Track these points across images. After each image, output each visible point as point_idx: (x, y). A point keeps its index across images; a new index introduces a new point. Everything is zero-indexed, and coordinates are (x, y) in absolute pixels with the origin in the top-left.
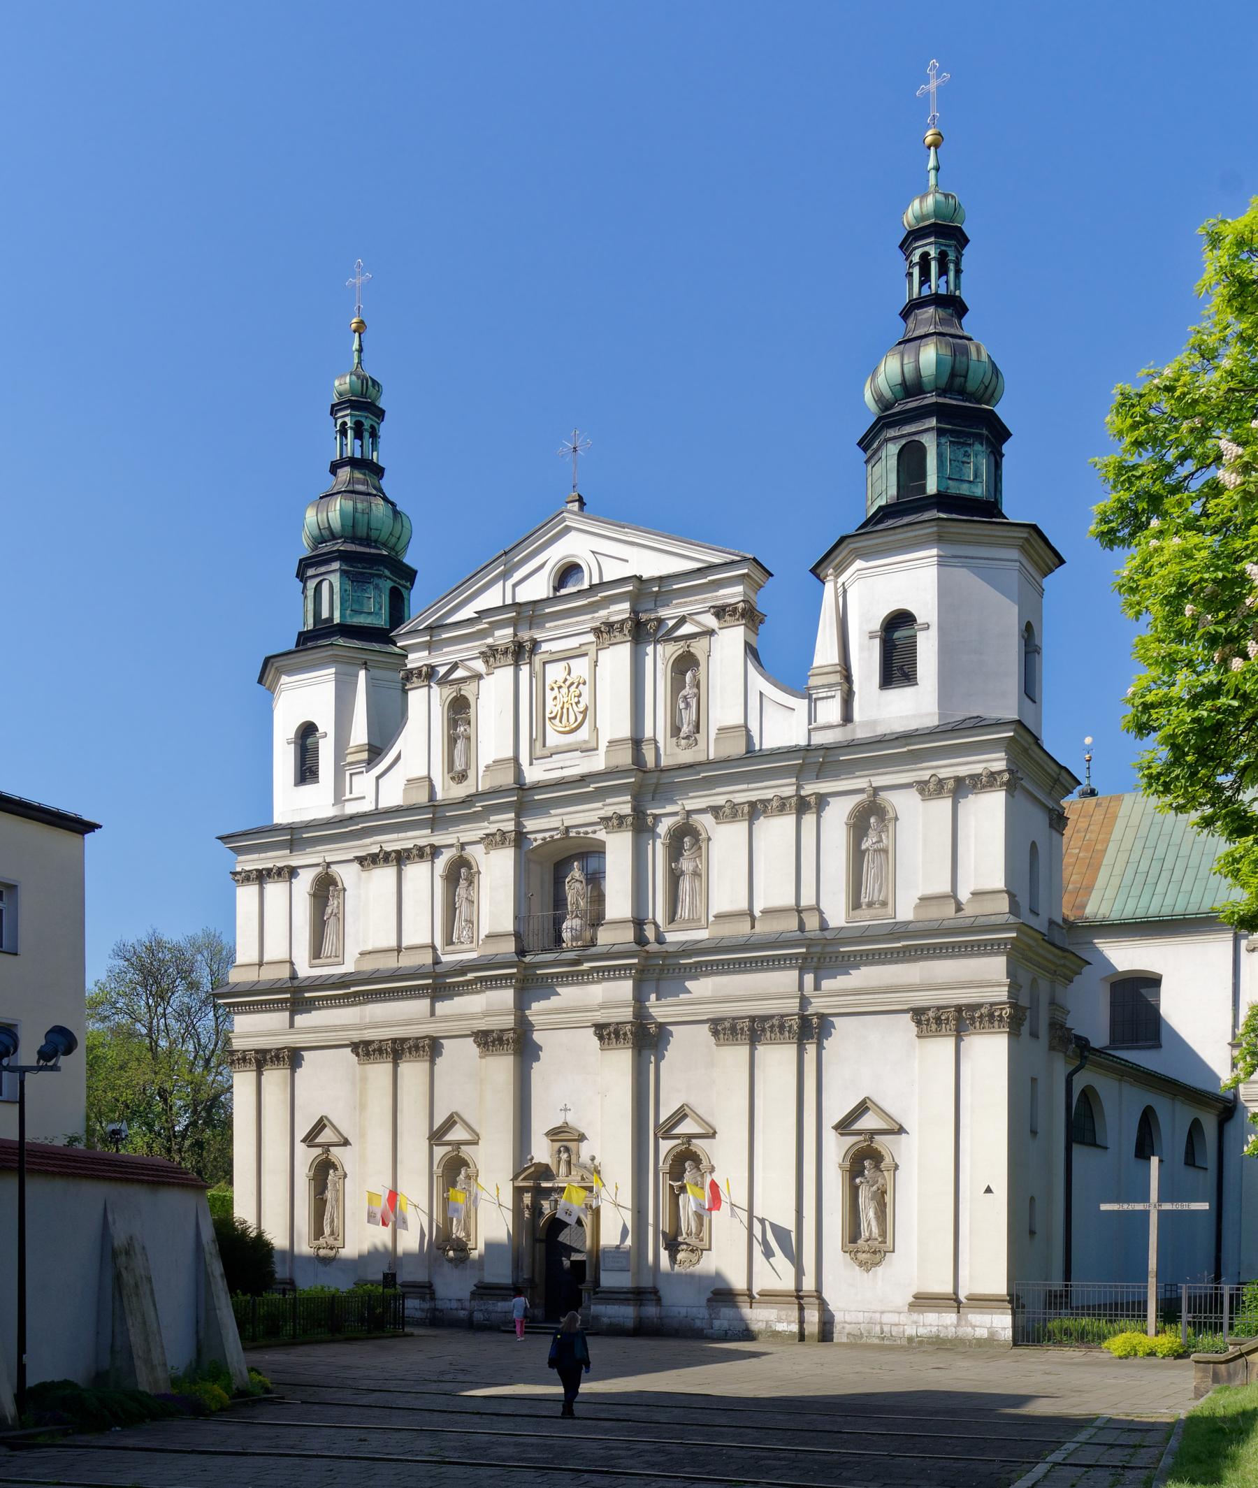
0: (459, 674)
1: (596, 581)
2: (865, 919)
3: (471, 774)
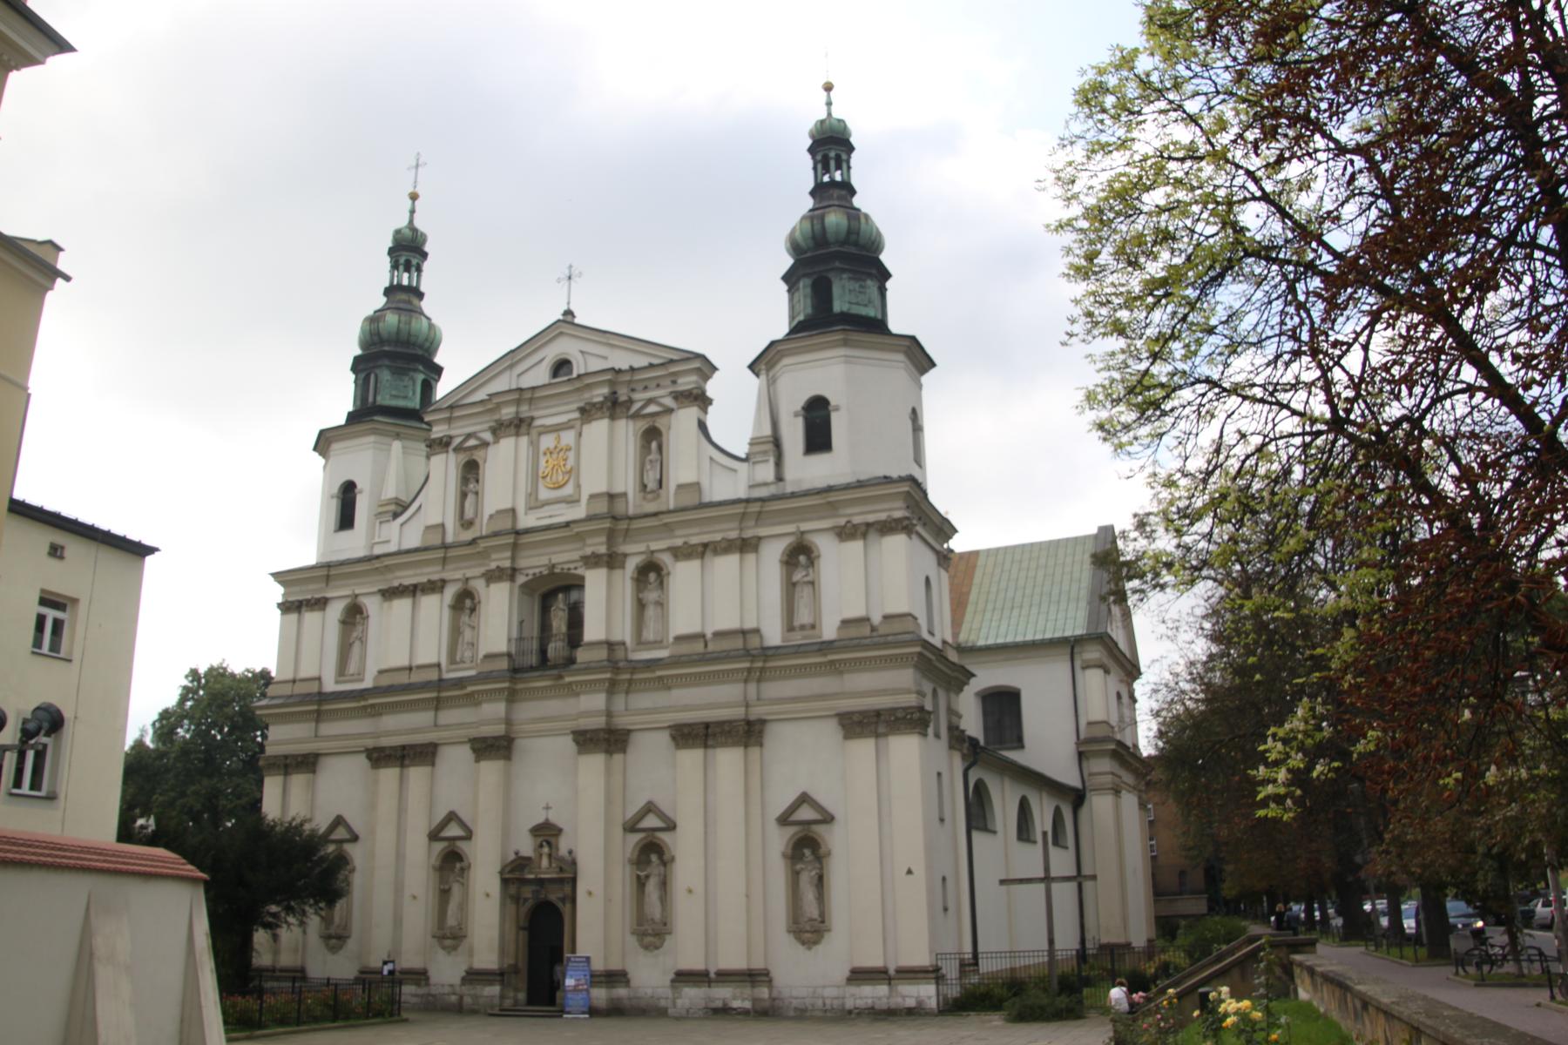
0: (472, 442)
1: (582, 371)
2: (797, 638)
3: (477, 522)
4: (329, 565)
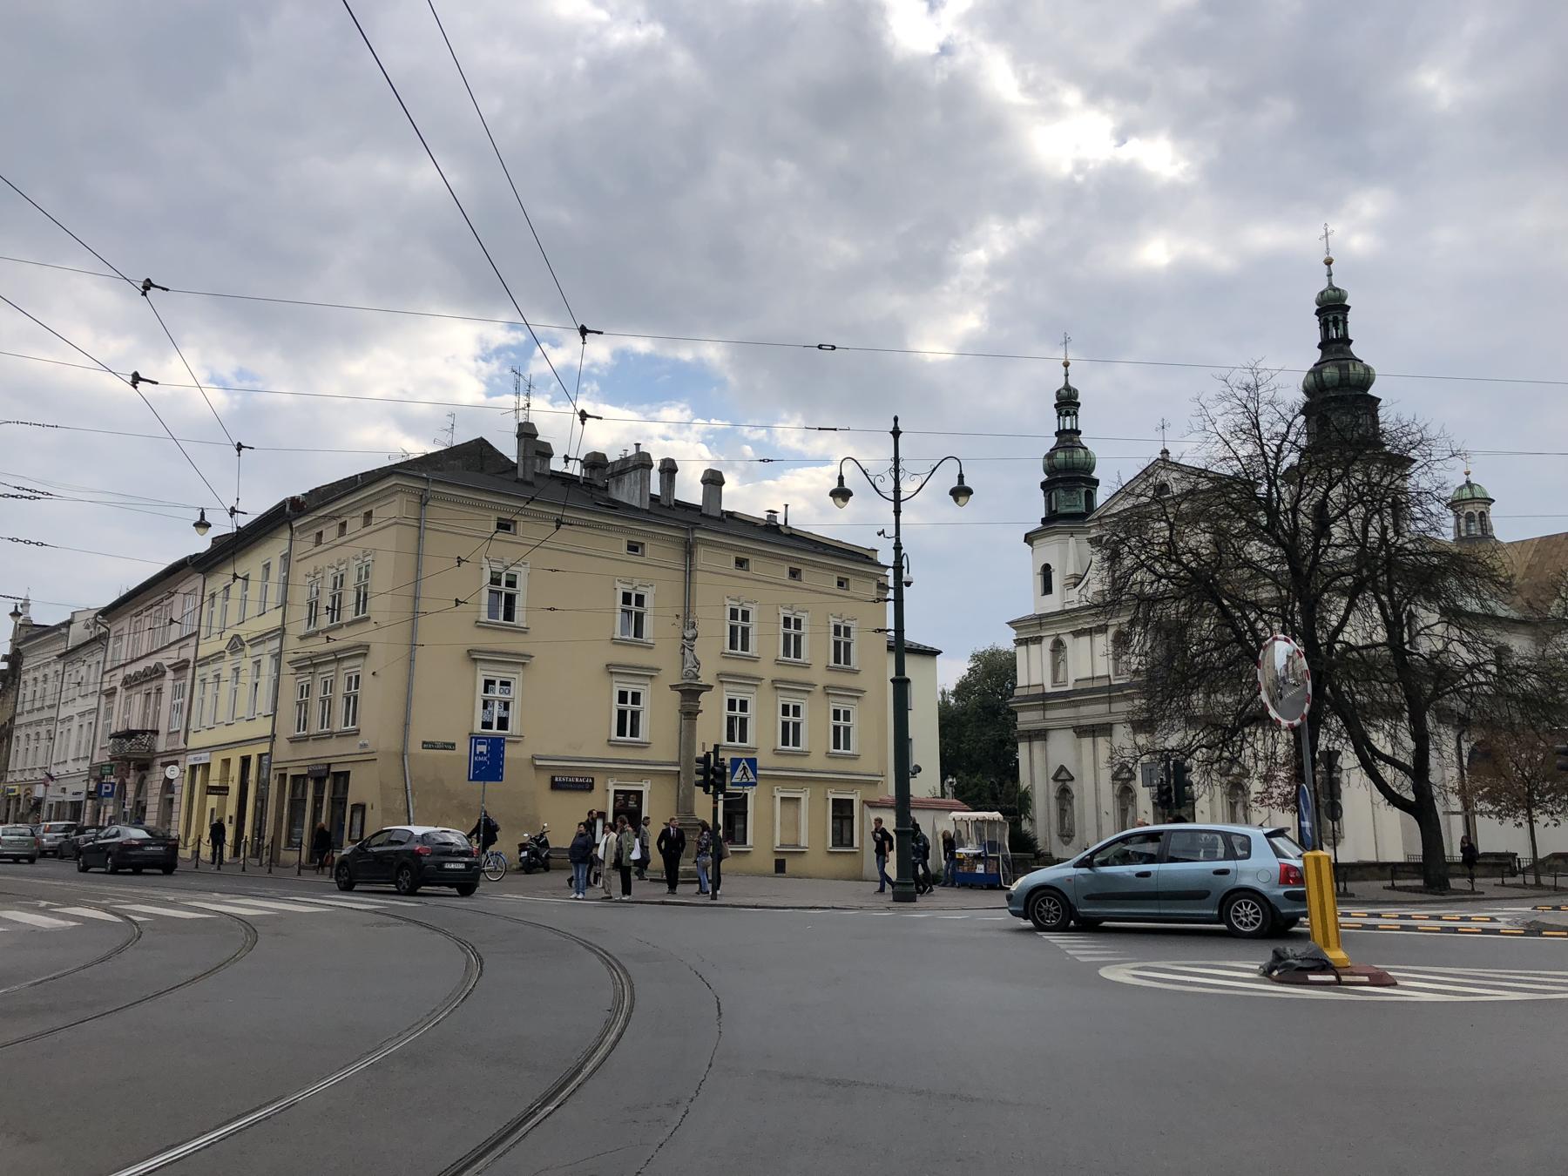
4: (1041, 617)
